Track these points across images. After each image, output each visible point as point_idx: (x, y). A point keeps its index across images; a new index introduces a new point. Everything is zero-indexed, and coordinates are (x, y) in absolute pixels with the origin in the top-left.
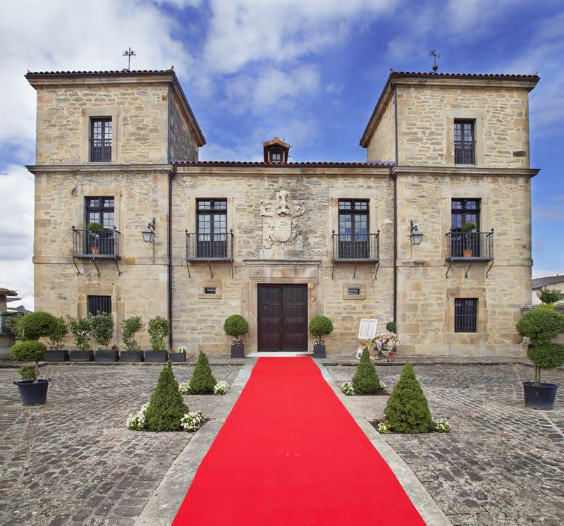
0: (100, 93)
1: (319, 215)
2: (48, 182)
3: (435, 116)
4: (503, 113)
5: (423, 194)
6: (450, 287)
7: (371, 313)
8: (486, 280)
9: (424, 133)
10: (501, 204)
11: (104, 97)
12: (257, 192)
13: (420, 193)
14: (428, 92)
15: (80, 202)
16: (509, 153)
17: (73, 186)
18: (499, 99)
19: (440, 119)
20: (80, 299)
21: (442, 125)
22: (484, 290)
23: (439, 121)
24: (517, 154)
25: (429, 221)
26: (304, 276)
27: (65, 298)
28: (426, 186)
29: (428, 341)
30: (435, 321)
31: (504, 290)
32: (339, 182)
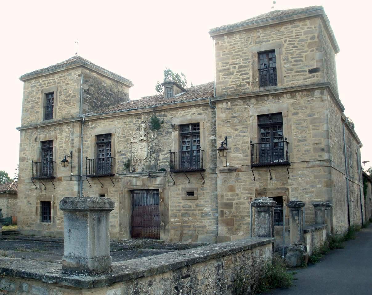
0: (50, 79)
1: (166, 138)
2: (25, 135)
3: (243, 53)
4: (298, 40)
5: (234, 115)
6: (258, 188)
7: (202, 210)
8: (289, 181)
9: (235, 68)
10: (300, 115)
11: (51, 81)
12: (129, 127)
13: (232, 114)
14: (237, 36)
15: (38, 146)
16: (305, 71)
17: (35, 136)
18: (294, 30)
19: (246, 55)
20: (37, 204)
21: (248, 59)
22: (288, 189)
23: (246, 56)
24: (311, 71)
25: (240, 136)
26: (157, 183)
27: (30, 204)
28: (236, 108)
29: (241, 233)
30: (246, 216)
31: (305, 189)
32: (179, 113)
